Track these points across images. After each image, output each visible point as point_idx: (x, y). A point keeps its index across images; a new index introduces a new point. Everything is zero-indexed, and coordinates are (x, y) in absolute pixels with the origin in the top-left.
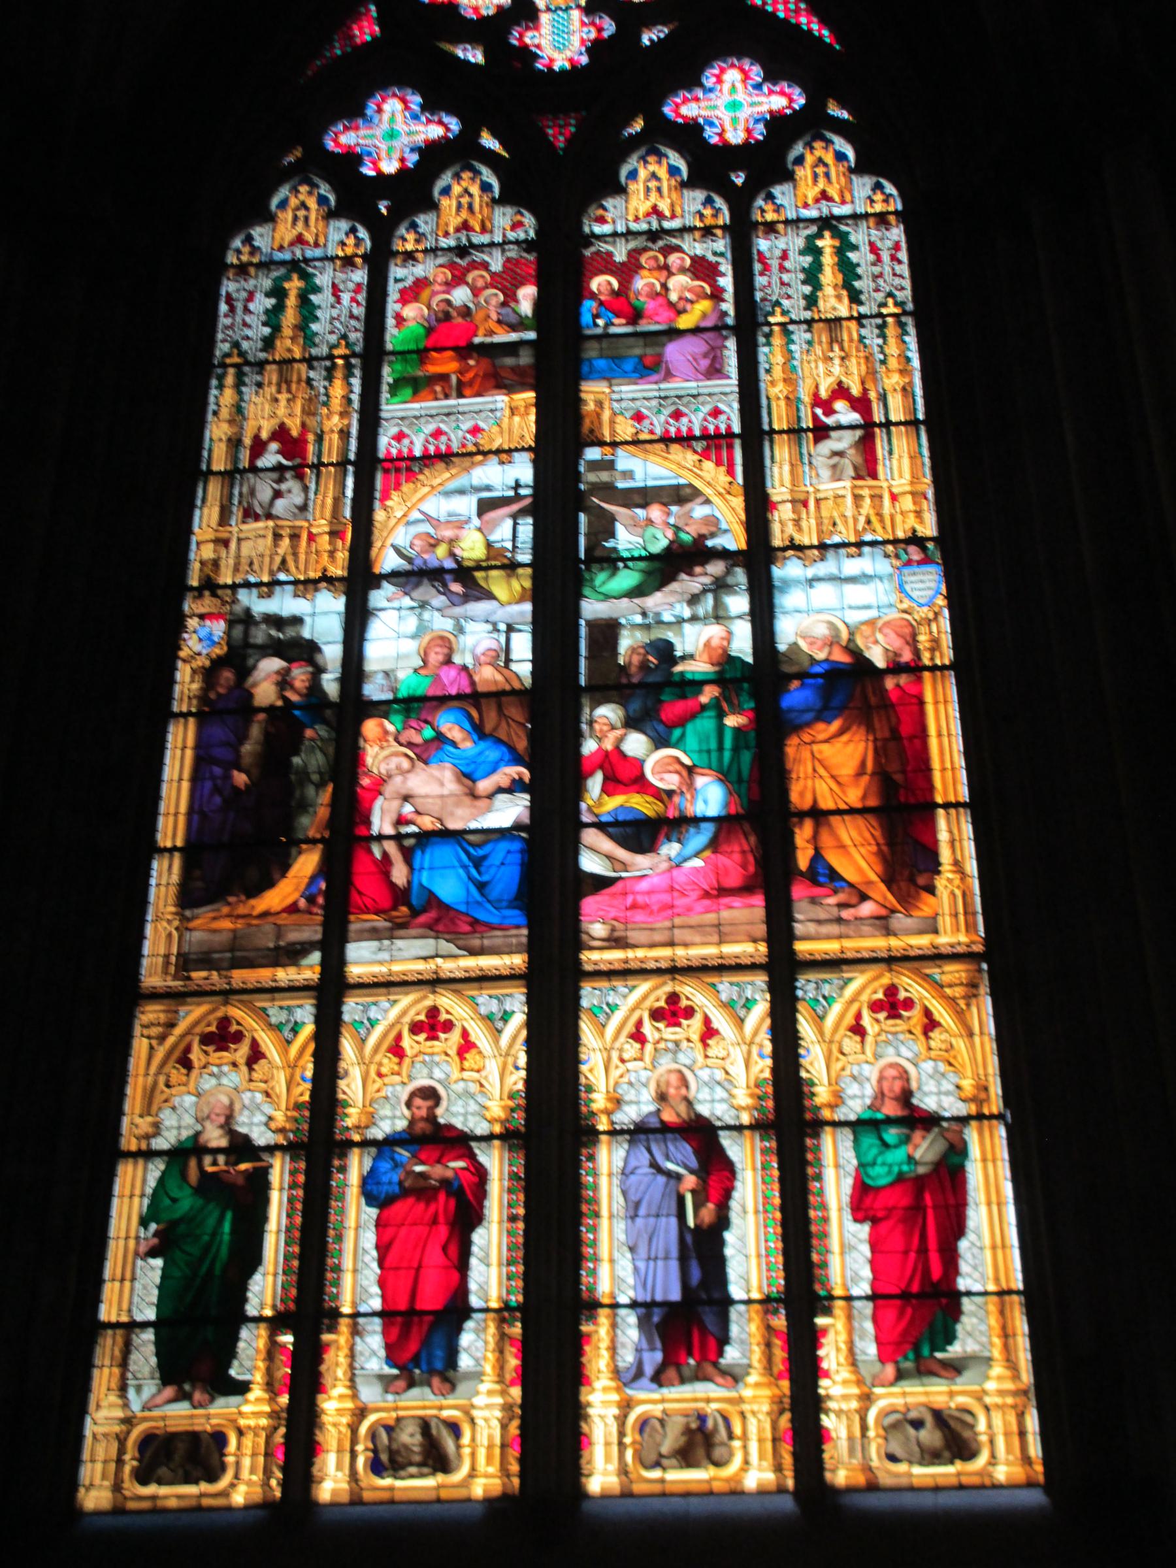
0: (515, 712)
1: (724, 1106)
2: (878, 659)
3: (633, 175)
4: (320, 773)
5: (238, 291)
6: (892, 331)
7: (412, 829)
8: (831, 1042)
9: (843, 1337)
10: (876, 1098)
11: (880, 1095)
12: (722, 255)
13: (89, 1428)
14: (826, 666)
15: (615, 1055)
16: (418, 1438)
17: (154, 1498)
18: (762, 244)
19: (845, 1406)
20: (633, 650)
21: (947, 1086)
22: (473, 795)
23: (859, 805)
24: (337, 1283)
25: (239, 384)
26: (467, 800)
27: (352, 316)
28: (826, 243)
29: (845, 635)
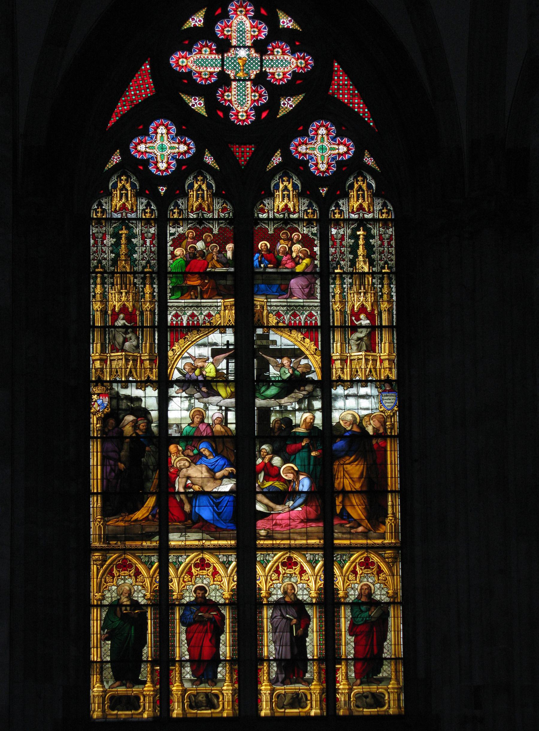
0: (230, 445)
1: (307, 597)
2: (370, 430)
3: (277, 187)
4: (154, 466)
5: (97, 233)
6: (386, 281)
7: (192, 490)
8: (345, 576)
9: (344, 671)
10: (359, 595)
11: (360, 595)
12: (315, 235)
13: (91, 694)
14: (350, 433)
15: (269, 578)
16: (205, 698)
17: (117, 714)
18: (334, 231)
19: (343, 691)
20: (276, 421)
21: (384, 592)
22: (214, 478)
23: (360, 490)
24: (174, 650)
25: (103, 283)
26: (212, 480)
27: (151, 252)
28: (361, 233)
29: (358, 420)
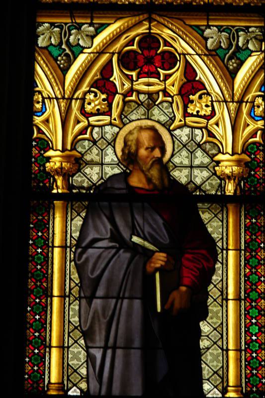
1: (205, 174)
15: (75, 105)
